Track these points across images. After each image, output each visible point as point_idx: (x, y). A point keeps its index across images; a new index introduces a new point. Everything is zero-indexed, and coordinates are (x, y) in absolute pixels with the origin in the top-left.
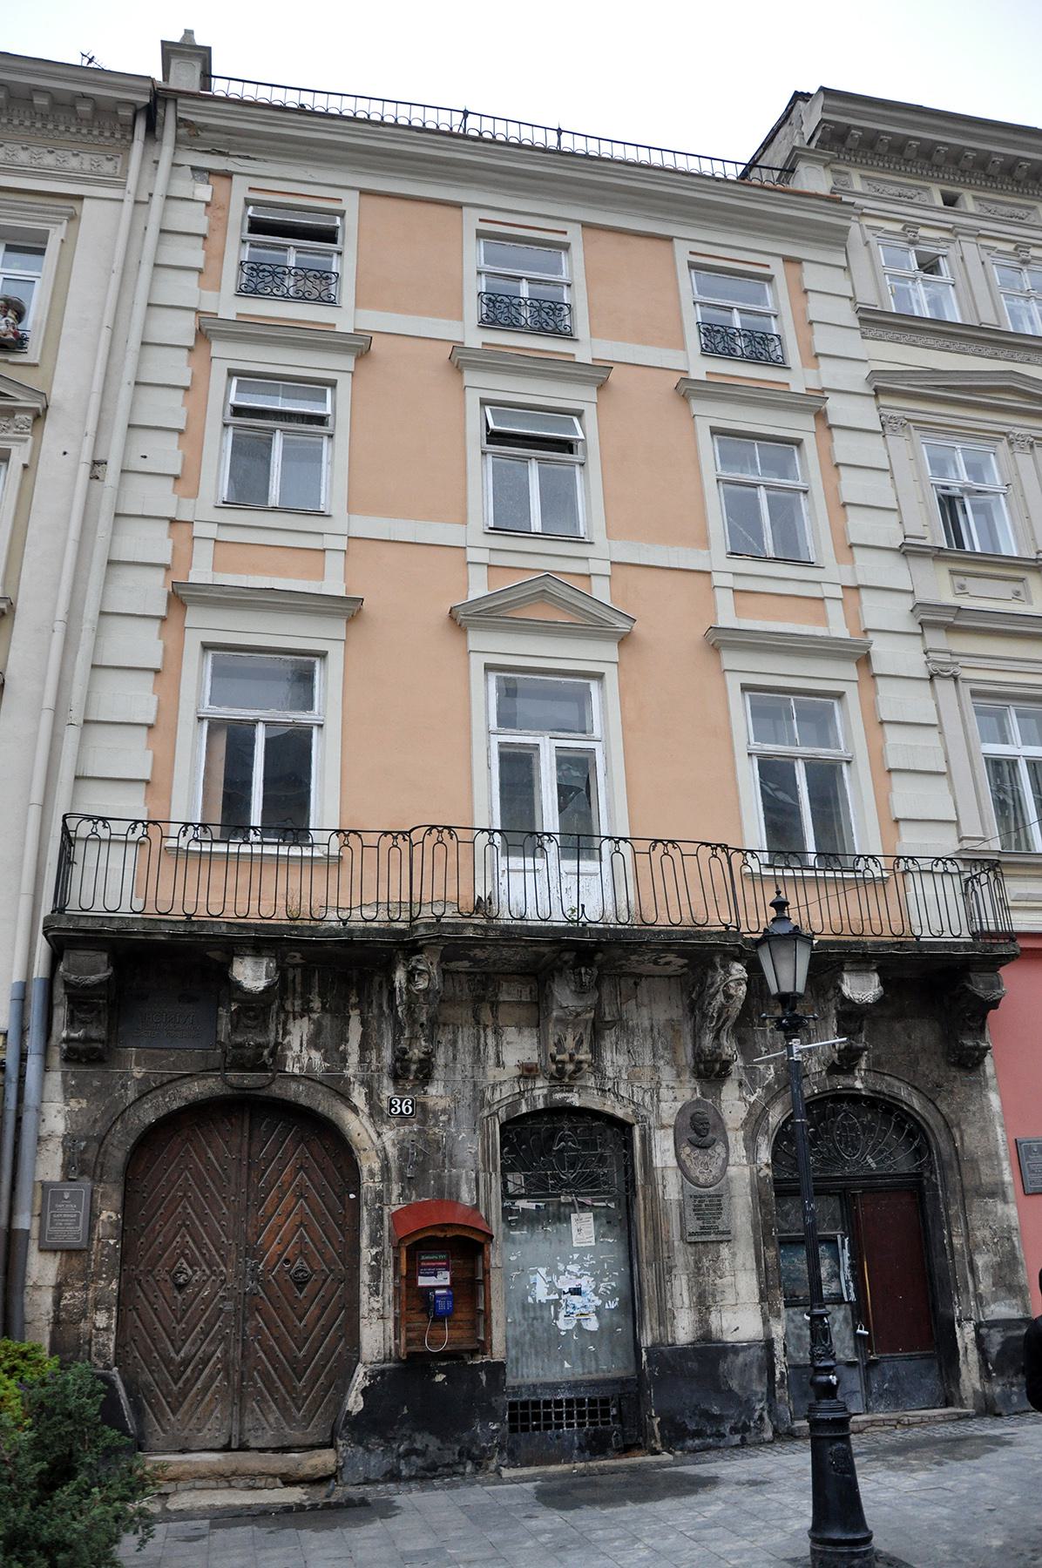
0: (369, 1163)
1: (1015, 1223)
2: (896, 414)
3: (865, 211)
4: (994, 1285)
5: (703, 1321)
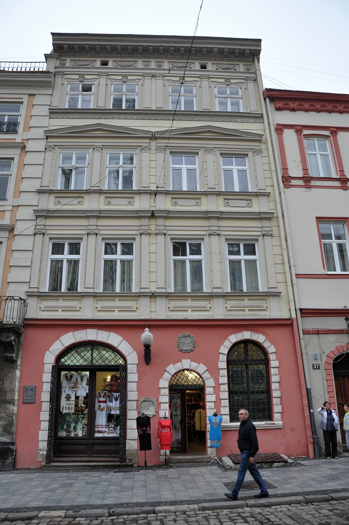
1: (15, 412)
2: (52, 144)
3: (65, 73)
4: (3, 431)
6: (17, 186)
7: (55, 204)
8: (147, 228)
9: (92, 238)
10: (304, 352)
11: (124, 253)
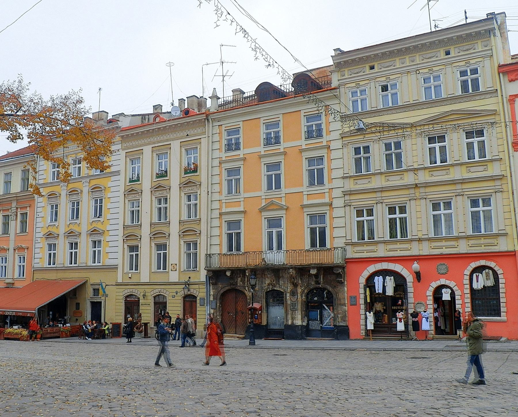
0: (248, 298)
1: (347, 310)
5: (293, 322)
8: (413, 195)
11: (401, 213)
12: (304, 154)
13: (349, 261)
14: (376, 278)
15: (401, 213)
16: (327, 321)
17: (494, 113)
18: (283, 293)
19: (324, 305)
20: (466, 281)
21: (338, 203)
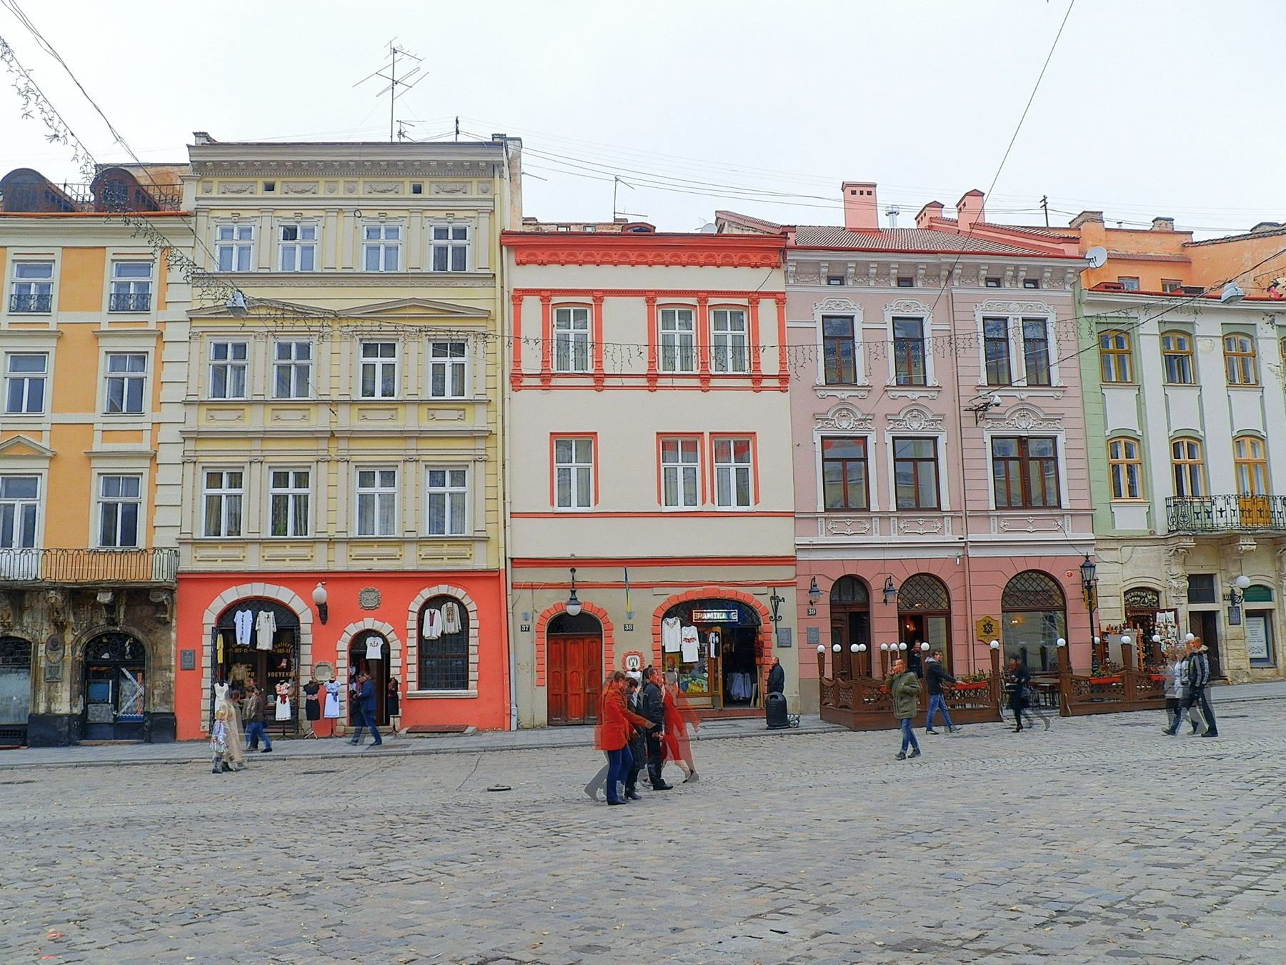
1: (172, 680)
5: (49, 707)
6: (156, 395)
7: (208, 420)
9: (256, 467)
10: (510, 610)
11: (298, 486)
12: (102, 342)
13: (184, 578)
14: (239, 614)
15: (298, 486)
16: (129, 704)
17: (486, 316)
18: (31, 643)
19: (124, 670)
20: (412, 624)
21: (171, 454)
